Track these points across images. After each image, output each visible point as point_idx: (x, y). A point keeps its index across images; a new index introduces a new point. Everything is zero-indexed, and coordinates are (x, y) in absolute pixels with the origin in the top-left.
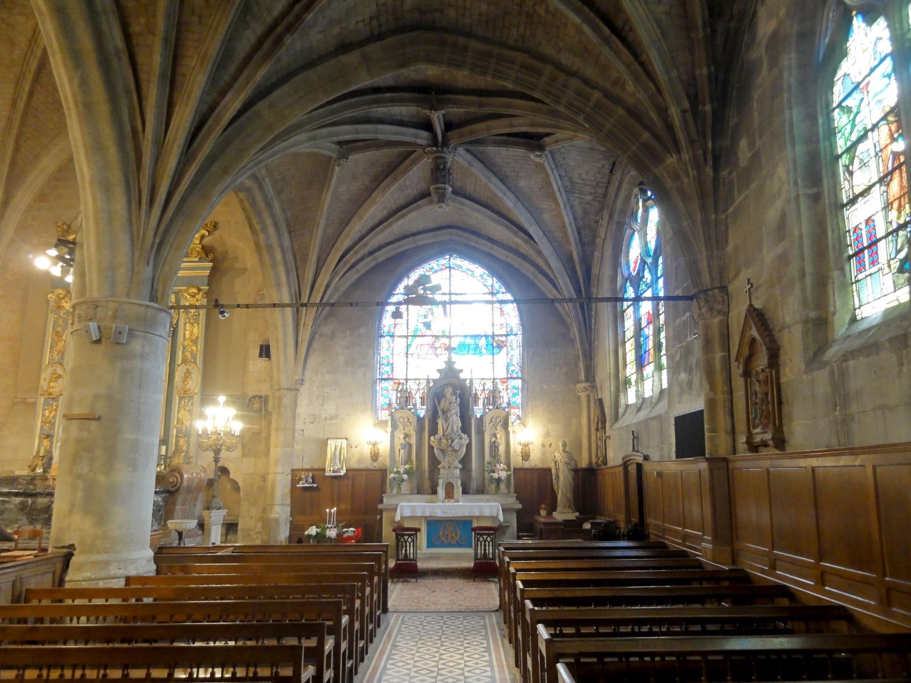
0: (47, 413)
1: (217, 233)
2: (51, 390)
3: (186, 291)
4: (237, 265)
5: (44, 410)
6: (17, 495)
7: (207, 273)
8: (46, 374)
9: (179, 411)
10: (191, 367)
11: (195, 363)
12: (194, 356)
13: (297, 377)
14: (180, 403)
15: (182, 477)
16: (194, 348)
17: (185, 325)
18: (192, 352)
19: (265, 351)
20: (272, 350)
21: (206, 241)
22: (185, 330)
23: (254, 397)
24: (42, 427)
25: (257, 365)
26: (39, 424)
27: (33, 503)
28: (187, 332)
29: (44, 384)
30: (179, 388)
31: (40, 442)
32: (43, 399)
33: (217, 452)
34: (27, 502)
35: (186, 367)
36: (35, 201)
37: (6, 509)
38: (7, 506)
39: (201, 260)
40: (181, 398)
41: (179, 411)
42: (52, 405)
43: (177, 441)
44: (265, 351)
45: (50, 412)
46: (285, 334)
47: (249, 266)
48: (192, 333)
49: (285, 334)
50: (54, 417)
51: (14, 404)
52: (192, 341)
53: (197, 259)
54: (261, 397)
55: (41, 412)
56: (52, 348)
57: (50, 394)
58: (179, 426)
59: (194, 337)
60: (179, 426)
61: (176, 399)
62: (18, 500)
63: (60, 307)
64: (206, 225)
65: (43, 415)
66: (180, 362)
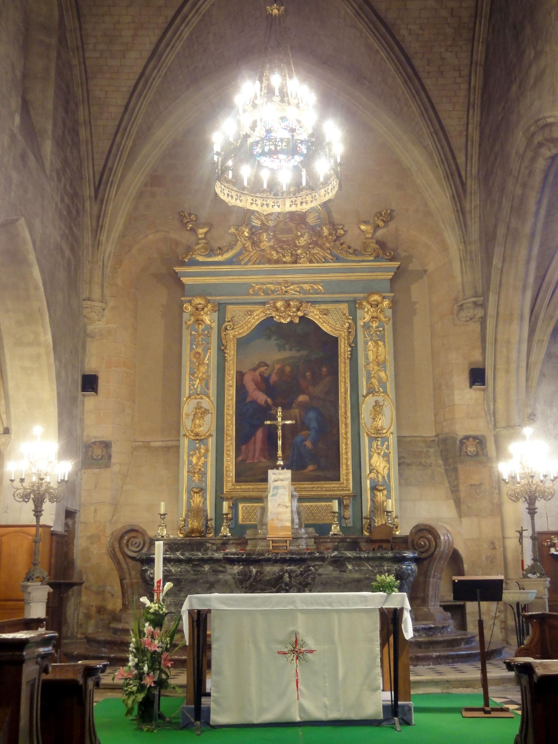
0: (194, 460)
1: (392, 225)
2: (197, 430)
3: (367, 299)
4: (411, 267)
5: (189, 455)
6: (232, 562)
7: (390, 275)
8: (188, 408)
9: (371, 457)
10: (380, 398)
11: (385, 392)
12: (383, 384)
13: (529, 411)
14: (370, 447)
15: (436, 537)
16: (382, 374)
17: (366, 343)
18: (380, 380)
19: (477, 376)
20: (489, 374)
21: (380, 233)
22: (366, 349)
23: (467, 438)
24: (190, 479)
25: (465, 396)
26: (186, 474)
27: (259, 573)
28: (370, 353)
29: (187, 423)
30: (369, 426)
31: (190, 497)
32: (186, 441)
33: (531, 501)
34: (251, 572)
36: (146, 185)
37: (218, 581)
38: (221, 576)
39: (377, 258)
40: (372, 439)
42: (199, 449)
43: (373, 496)
44: (477, 376)
45: (199, 458)
46: (519, 352)
47: (431, 267)
49: (519, 352)
50: (205, 464)
51: (135, 449)
52: (378, 364)
53: (371, 258)
54: (475, 438)
55: (186, 457)
56: (192, 374)
57: (197, 434)
58: (372, 475)
59: (381, 358)
60: (372, 475)
61: (365, 441)
62: (237, 569)
63: (199, 321)
65: (190, 462)
66: (365, 393)
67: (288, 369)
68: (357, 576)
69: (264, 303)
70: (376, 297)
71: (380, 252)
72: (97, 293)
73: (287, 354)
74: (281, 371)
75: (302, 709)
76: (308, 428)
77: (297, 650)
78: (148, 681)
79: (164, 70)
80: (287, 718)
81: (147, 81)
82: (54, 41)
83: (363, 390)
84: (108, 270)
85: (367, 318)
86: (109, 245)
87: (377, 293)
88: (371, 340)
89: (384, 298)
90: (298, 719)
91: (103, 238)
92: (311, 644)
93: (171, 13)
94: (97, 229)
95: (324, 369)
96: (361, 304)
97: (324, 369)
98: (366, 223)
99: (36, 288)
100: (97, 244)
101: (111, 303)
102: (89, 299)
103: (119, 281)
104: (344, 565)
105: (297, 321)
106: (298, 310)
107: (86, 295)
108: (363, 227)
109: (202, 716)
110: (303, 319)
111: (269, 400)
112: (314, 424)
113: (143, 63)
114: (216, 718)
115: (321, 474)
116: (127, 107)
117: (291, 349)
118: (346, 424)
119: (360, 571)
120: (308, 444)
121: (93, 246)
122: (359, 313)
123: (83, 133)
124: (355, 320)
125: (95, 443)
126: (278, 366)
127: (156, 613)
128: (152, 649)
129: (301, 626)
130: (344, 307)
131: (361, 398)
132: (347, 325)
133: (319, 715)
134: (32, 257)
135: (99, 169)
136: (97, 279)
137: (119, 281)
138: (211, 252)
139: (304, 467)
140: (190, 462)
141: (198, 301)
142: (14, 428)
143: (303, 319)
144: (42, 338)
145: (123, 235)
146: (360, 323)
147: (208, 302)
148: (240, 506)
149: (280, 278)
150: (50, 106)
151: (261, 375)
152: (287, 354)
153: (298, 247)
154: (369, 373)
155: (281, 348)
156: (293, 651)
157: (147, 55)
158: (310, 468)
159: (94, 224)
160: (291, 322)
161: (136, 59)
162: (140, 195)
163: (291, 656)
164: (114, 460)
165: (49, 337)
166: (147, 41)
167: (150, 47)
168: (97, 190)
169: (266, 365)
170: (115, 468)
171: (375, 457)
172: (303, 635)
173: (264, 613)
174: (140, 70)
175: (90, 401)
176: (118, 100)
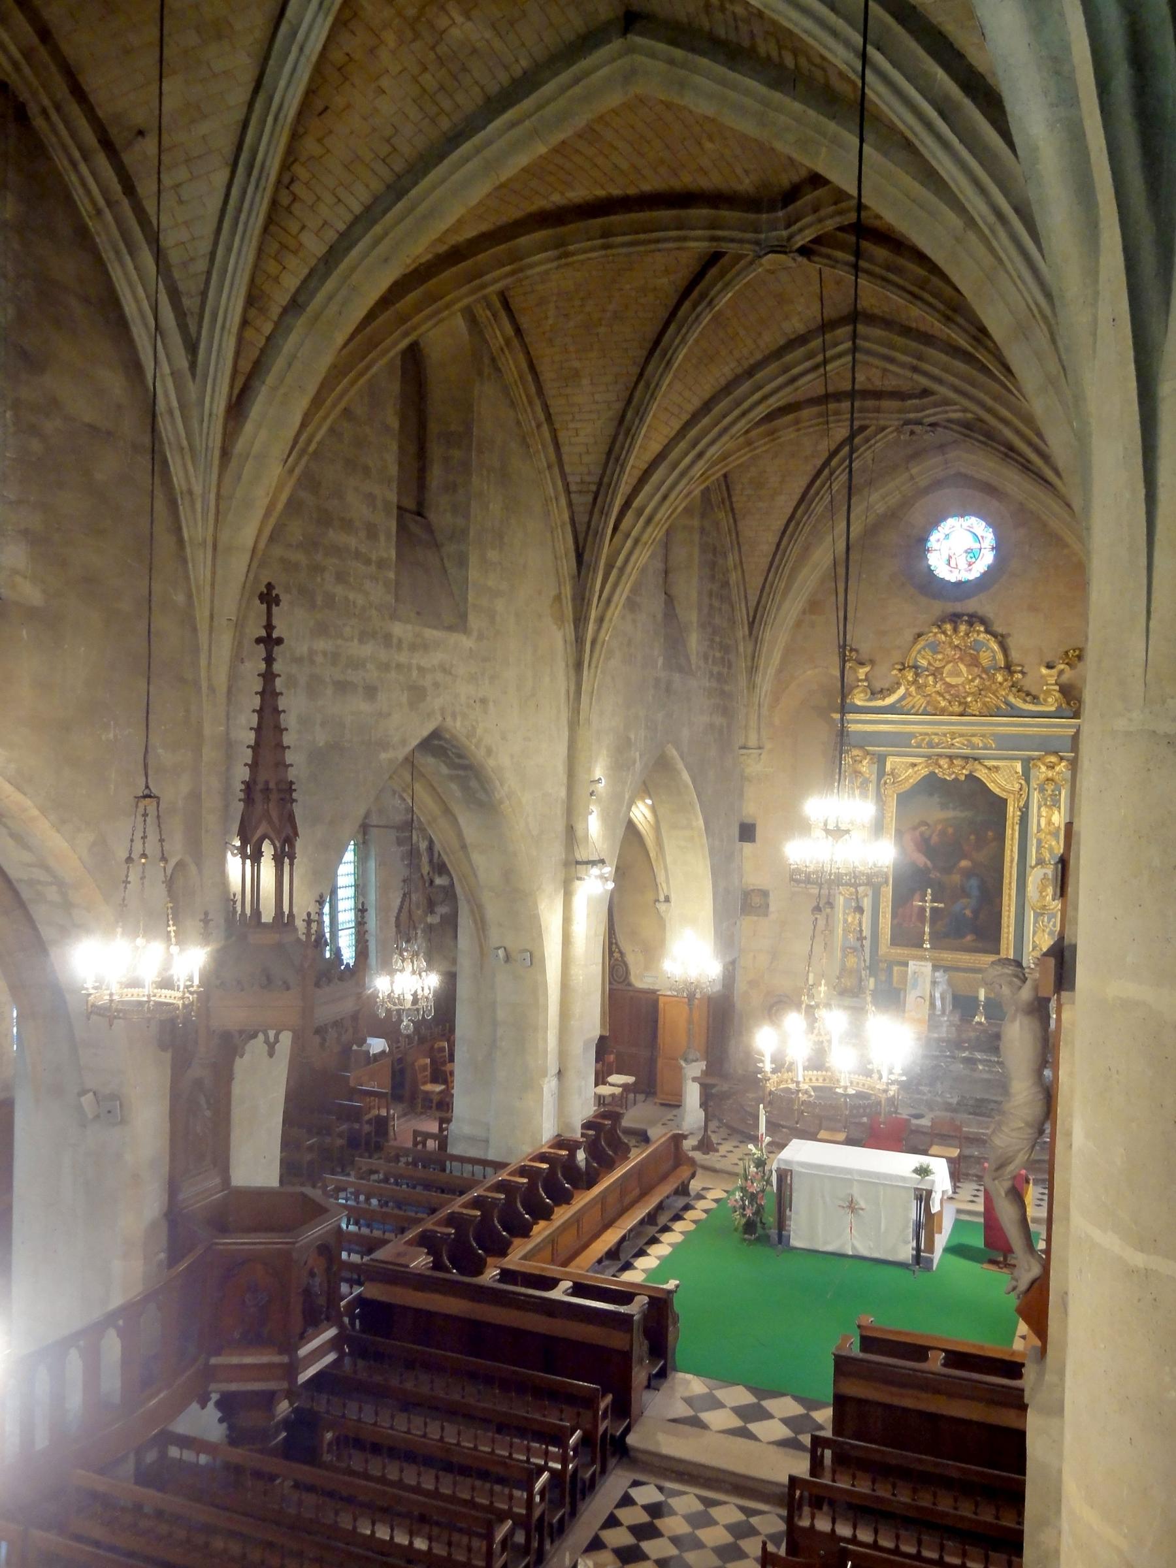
0: (850, 920)
5: (844, 913)
14: (1036, 922)
21: (1064, 678)
22: (1039, 816)
31: (845, 956)
32: (842, 898)
35: (1044, 871)
36: (804, 612)
40: (1037, 915)
41: (1035, 933)
48: (1049, 823)
52: (1050, 833)
59: (1052, 828)
61: (1030, 917)
64: (1066, 653)
65: (845, 921)
66: (1034, 863)
67: (950, 830)
68: (986, 1076)
69: (929, 757)
70: (1053, 759)
71: (1063, 701)
72: (753, 741)
73: (950, 814)
74: (943, 833)
75: (853, 1247)
76: (968, 896)
77: (852, 1207)
78: (749, 1213)
79: (813, 519)
80: (843, 1251)
81: (798, 524)
82: (696, 523)
83: (1032, 859)
84: (765, 711)
85: (1042, 777)
86: (766, 681)
87: (1056, 753)
88: (1045, 804)
89: (1062, 759)
90: (850, 1253)
91: (758, 680)
92: (862, 1204)
93: (819, 463)
94: (753, 669)
95: (990, 834)
96: (1035, 766)
97: (990, 834)
98: (1050, 666)
99: (686, 786)
100: (752, 686)
101: (768, 746)
102: (744, 748)
103: (777, 721)
104: (975, 1064)
105: (963, 778)
106: (964, 768)
107: (741, 742)
108: (1044, 671)
109: (784, 1239)
110: (971, 777)
111: (929, 863)
112: (975, 893)
113: (794, 503)
114: (795, 1242)
115: (980, 945)
116: (778, 545)
117: (954, 809)
118: (1010, 895)
119: (990, 1072)
120: (968, 912)
121: (748, 688)
122: (1033, 772)
123: (734, 577)
124: (1028, 781)
125: (753, 890)
126: (939, 827)
127: (759, 1159)
128: (751, 1190)
129: (856, 1191)
130: (1018, 766)
131: (1028, 869)
132: (1017, 786)
133: (865, 1252)
134: (680, 765)
135: (753, 603)
136: (753, 724)
137: (777, 721)
138: (874, 694)
139: (963, 937)
140: (845, 921)
141: (855, 752)
142: (673, 898)
143: (971, 777)
144: (694, 824)
145: (780, 671)
146: (1034, 784)
147: (868, 753)
148: (895, 969)
149: (945, 728)
150: (694, 595)
151: (922, 834)
152: (950, 814)
153: (969, 694)
154: (1039, 841)
155: (944, 806)
156: (849, 1207)
157: (797, 497)
158: (969, 938)
159: (749, 664)
160: (956, 779)
161: (785, 503)
162: (798, 624)
163: (848, 1210)
164: (772, 908)
165: (701, 822)
166: (797, 486)
167: (798, 492)
168: (751, 624)
169: (927, 824)
170: (773, 916)
171: (1040, 933)
172: (857, 1197)
173: (831, 1178)
174: (790, 510)
175: (748, 847)
176: (766, 541)
